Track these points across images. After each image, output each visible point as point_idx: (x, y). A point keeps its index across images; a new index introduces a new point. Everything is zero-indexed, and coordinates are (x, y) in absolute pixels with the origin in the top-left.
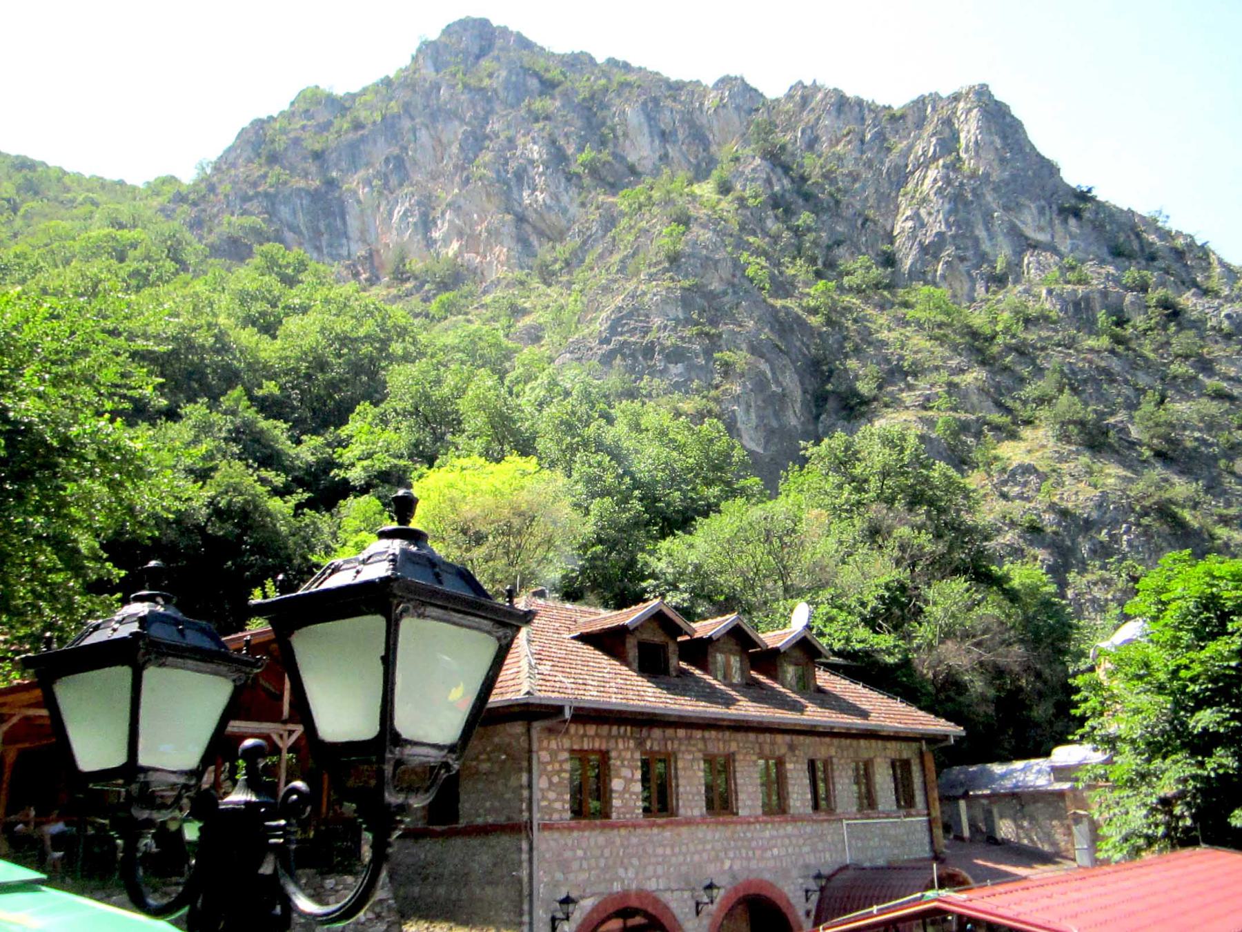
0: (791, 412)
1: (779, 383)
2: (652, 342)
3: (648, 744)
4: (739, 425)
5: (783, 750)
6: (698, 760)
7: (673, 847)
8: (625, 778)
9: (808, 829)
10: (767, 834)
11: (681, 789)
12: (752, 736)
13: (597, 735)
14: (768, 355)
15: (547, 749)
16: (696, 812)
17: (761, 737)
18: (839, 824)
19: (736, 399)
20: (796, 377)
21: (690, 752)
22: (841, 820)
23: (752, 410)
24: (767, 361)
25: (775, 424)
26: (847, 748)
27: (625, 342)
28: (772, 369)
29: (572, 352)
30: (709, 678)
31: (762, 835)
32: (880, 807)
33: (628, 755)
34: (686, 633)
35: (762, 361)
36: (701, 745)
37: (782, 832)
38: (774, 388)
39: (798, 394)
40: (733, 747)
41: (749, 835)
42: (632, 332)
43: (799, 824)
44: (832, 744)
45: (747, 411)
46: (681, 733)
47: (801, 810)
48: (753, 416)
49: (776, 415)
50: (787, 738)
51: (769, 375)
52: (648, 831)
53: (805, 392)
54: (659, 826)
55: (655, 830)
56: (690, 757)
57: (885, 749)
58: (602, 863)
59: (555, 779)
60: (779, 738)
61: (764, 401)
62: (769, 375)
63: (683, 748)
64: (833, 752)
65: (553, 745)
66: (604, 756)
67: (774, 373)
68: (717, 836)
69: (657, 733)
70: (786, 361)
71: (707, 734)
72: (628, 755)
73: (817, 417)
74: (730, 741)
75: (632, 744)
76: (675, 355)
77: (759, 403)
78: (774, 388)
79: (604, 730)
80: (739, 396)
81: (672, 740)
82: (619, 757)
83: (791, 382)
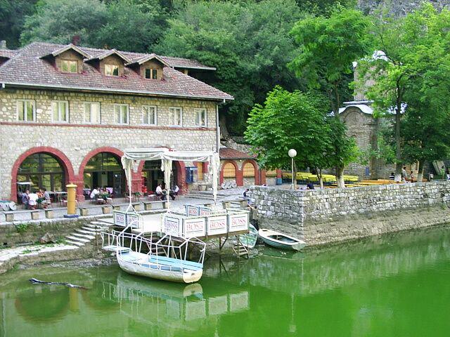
7: (66, 134)
8: (43, 109)
13: (30, 94)
15: (6, 98)
33: (45, 101)
34: (86, 58)
46: (71, 94)
55: (57, 127)
58: (31, 136)
59: (10, 108)
65: (9, 97)
71: (86, 95)
72: (45, 101)
75: (47, 97)
79: (34, 92)
82: (41, 102)
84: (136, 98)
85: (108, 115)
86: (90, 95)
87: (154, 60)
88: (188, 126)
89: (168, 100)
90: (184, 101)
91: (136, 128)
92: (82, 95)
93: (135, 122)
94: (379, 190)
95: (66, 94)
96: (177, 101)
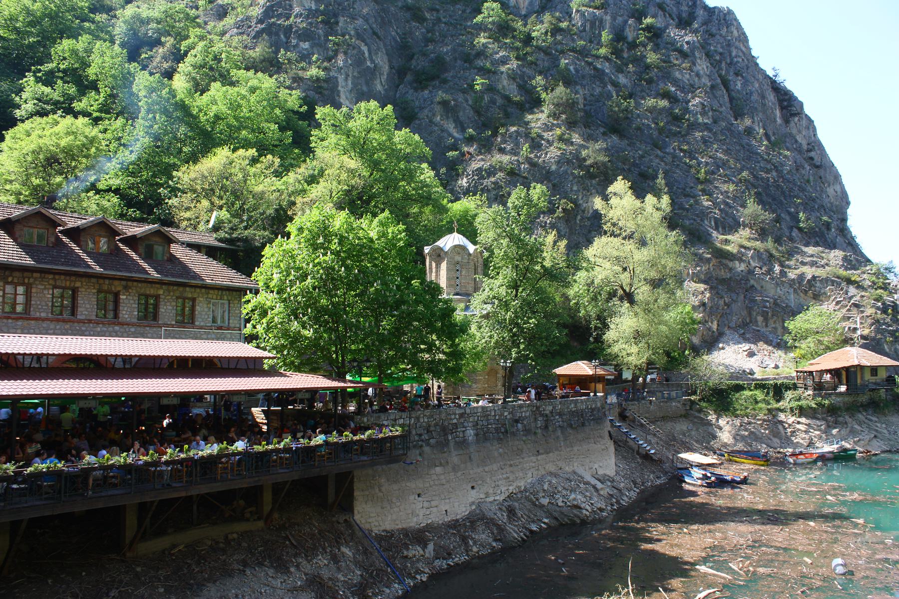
0: (378, 81)
1: (372, 61)
2: (291, 25)
3: (10, 279)
4: (340, 88)
5: (119, 289)
6: (48, 289)
9: (133, 330)
10: (99, 329)
11: (33, 302)
12: (93, 280)
14: (368, 41)
16: (43, 315)
17: (101, 281)
18: (160, 329)
19: (340, 69)
20: (385, 58)
21: (42, 285)
22: (161, 327)
23: (350, 79)
24: (366, 44)
25: (365, 89)
26: (174, 291)
27: (274, 24)
28: (369, 51)
29: (238, 28)
30: (77, 250)
31: (94, 329)
32: (197, 323)
34: (60, 226)
35: (363, 44)
36: (51, 282)
37: (111, 329)
38: (369, 63)
39: (386, 69)
40: (78, 284)
41: (83, 329)
42: (279, 17)
43: (125, 326)
44: (162, 288)
45: (346, 79)
46: (35, 275)
47: (128, 319)
48: (350, 82)
49: (367, 83)
50: (124, 283)
51: (367, 55)
52: (5, 321)
53: (391, 67)
54: (14, 319)
55: (10, 321)
56: (43, 287)
57: (208, 293)
60: (116, 283)
61: (359, 73)
62: (367, 55)
63: (37, 282)
64: (161, 292)
66: (157, 297)
67: (370, 53)
68: (58, 327)
69: (17, 274)
70: (381, 45)
71: (57, 277)
73: (398, 86)
74: (75, 281)
76: (305, 35)
77: (355, 74)
78: (369, 63)
80: (341, 68)
81: (29, 278)
83: (382, 61)
84: (130, 283)
85: (88, 306)
86: (63, 277)
87: (158, 233)
88: (202, 324)
89: (175, 288)
90: (198, 290)
91: (128, 324)
92: (51, 276)
93: (127, 316)
94: (455, 414)
95: (26, 274)
96: (188, 289)
